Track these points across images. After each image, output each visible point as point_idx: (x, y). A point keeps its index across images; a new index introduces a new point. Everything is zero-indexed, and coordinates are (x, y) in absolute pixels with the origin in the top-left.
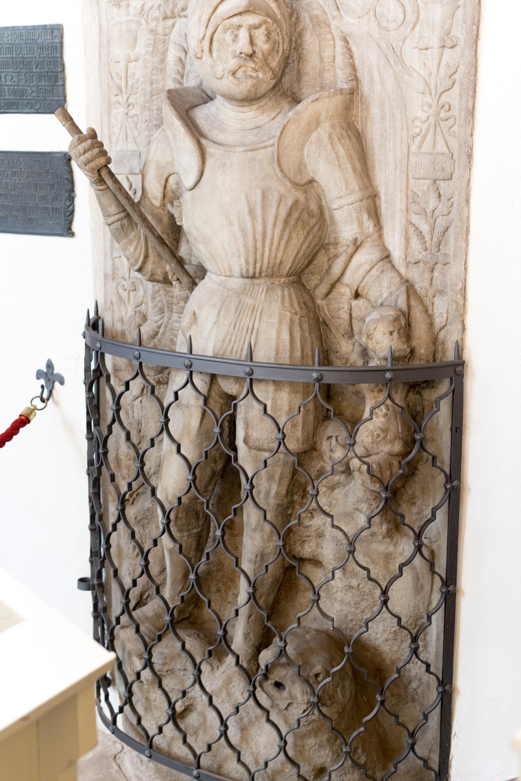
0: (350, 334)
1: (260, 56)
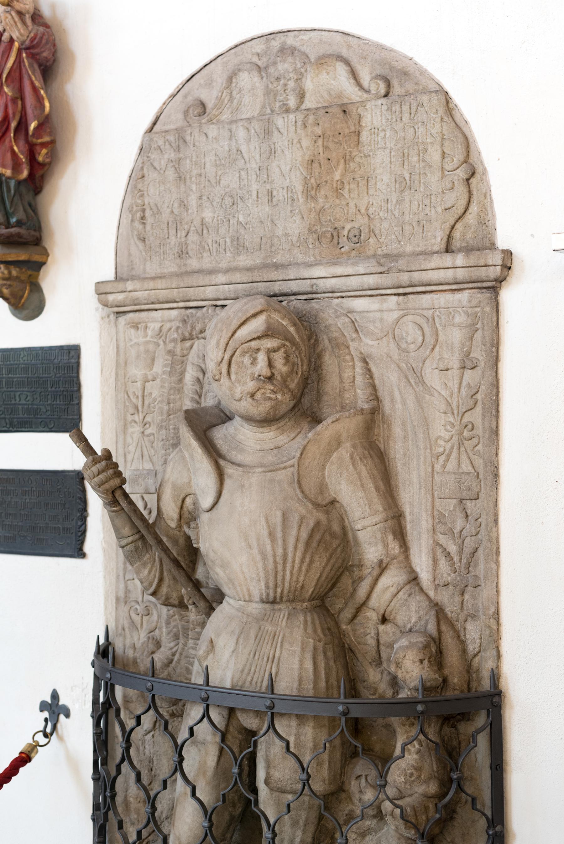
0: (378, 661)
1: (279, 378)
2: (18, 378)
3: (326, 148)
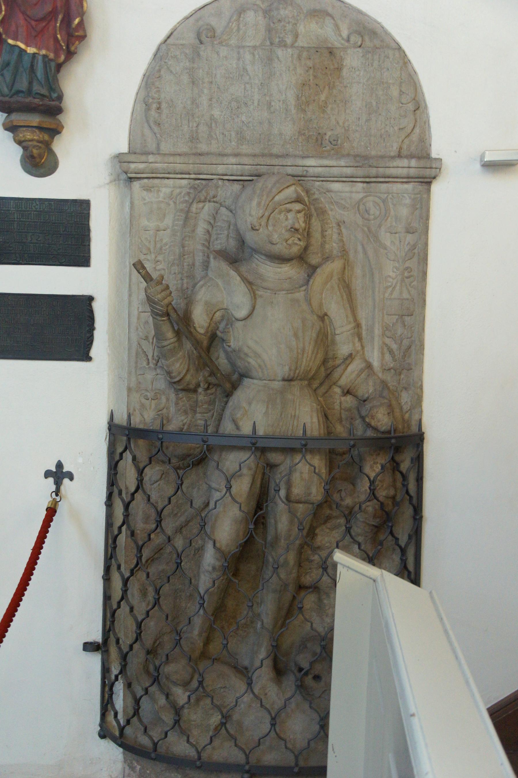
2: (29, 222)
3: (315, 77)
